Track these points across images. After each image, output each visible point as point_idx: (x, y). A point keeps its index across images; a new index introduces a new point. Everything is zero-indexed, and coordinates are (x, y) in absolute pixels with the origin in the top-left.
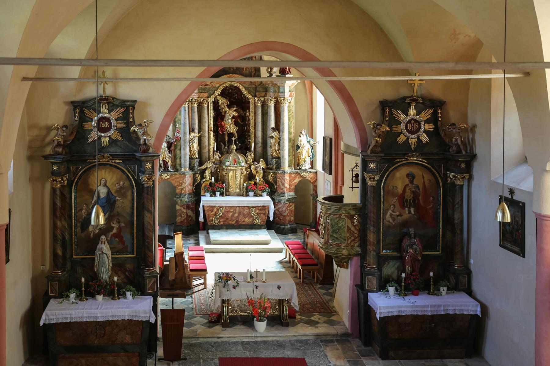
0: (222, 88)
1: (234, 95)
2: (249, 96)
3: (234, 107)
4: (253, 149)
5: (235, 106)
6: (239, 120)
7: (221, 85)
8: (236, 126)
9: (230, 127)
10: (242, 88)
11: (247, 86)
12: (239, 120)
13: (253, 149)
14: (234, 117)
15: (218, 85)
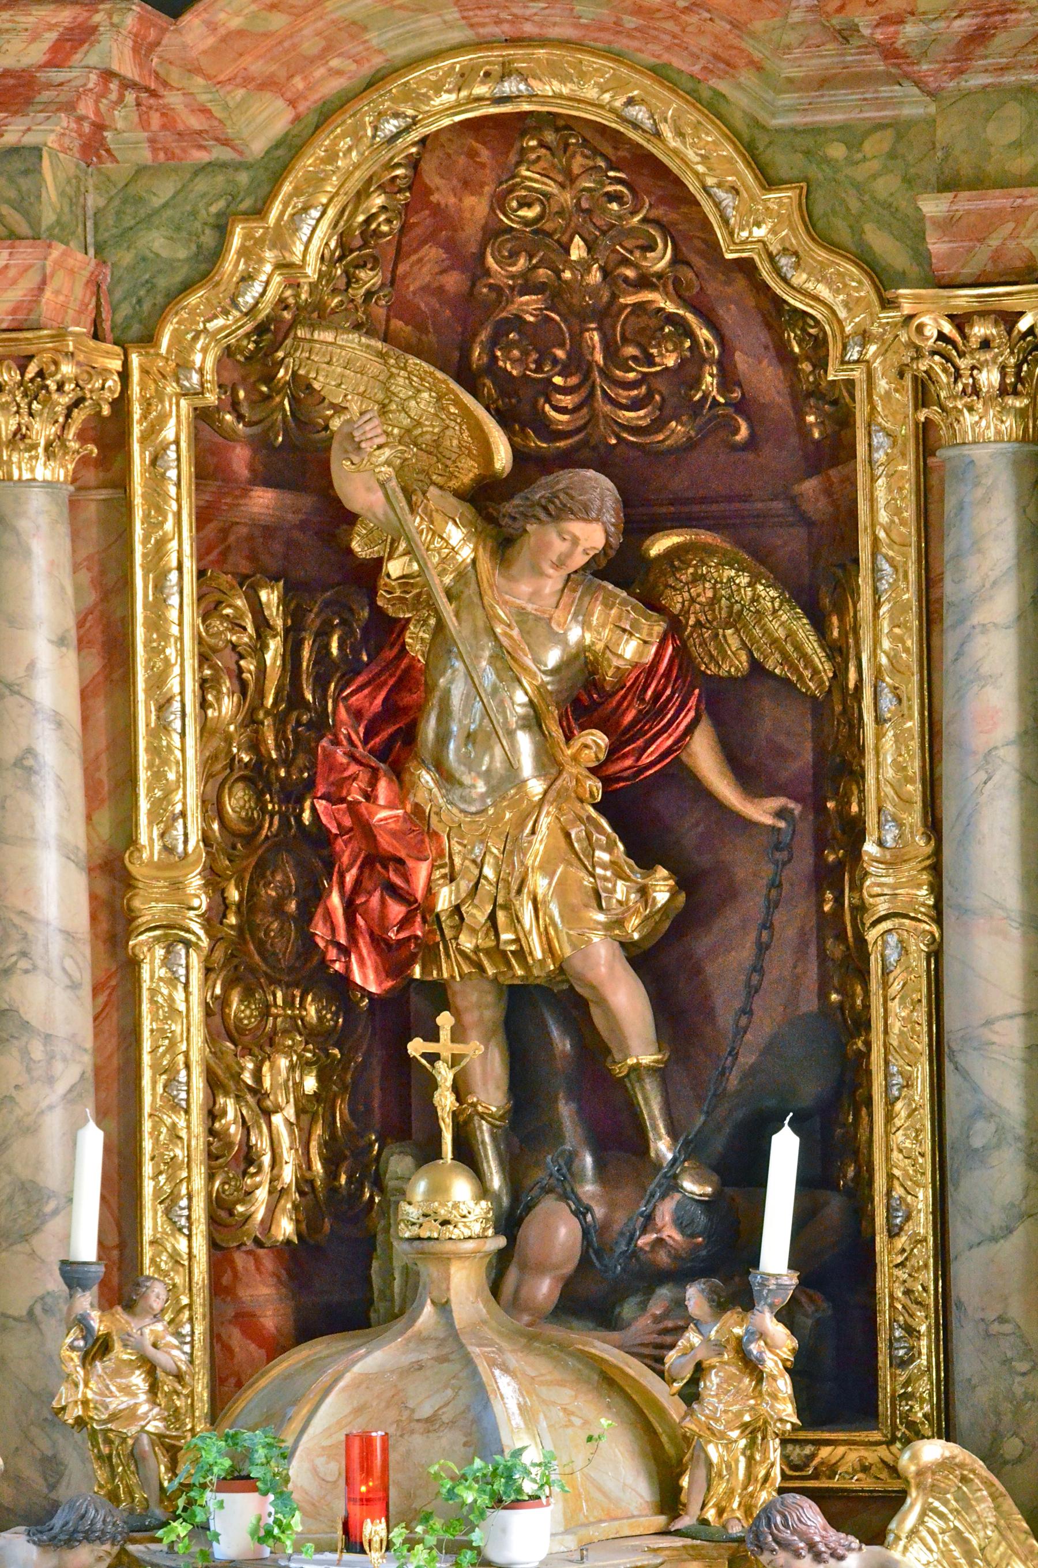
0: (344, 158)
1: (652, 327)
2: (825, 291)
3: (557, 511)
4: (775, 1253)
5: (599, 487)
6: (704, 756)
7: (327, 114)
8: (644, 849)
9: (520, 860)
10: (697, 152)
11: (786, 114)
12: (704, 756)
13: (775, 1253)
14: (585, 697)
15: (264, 123)
